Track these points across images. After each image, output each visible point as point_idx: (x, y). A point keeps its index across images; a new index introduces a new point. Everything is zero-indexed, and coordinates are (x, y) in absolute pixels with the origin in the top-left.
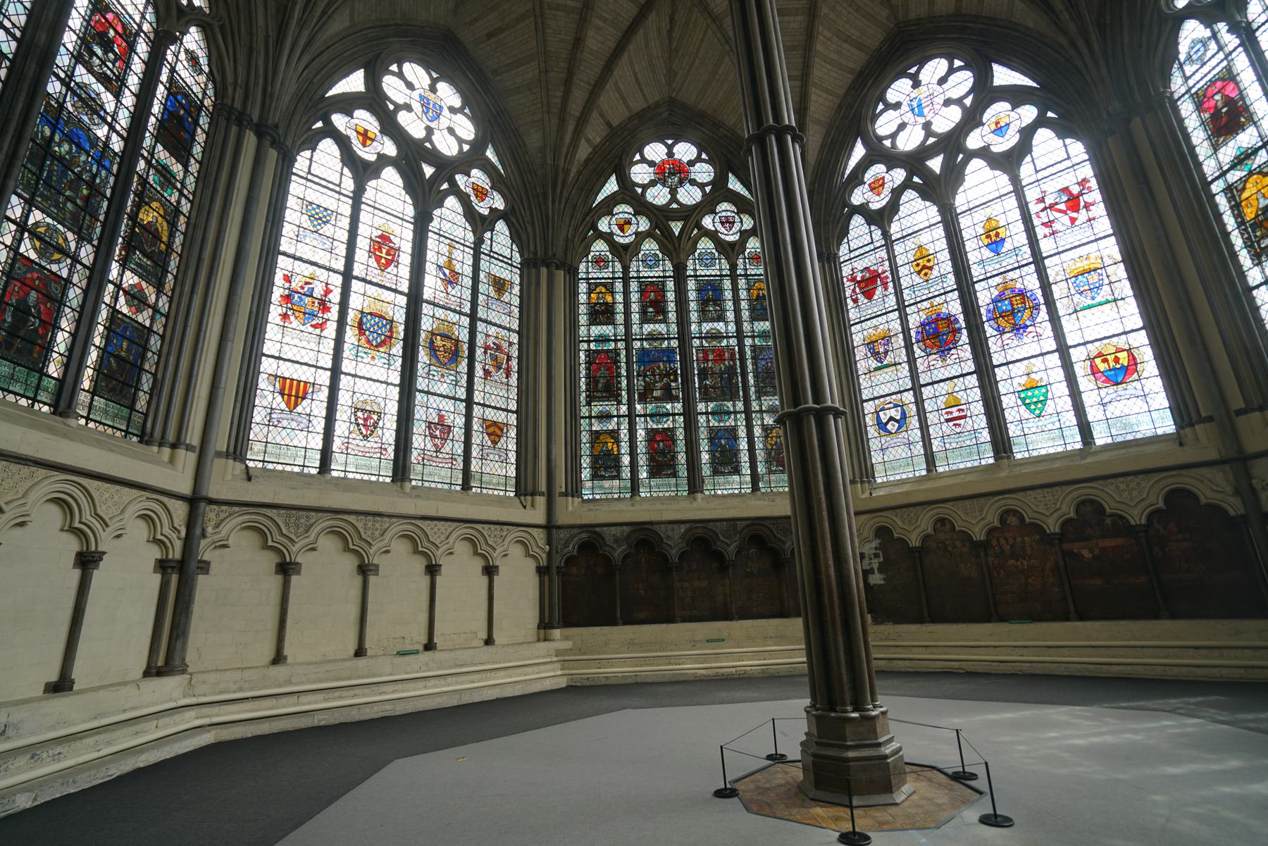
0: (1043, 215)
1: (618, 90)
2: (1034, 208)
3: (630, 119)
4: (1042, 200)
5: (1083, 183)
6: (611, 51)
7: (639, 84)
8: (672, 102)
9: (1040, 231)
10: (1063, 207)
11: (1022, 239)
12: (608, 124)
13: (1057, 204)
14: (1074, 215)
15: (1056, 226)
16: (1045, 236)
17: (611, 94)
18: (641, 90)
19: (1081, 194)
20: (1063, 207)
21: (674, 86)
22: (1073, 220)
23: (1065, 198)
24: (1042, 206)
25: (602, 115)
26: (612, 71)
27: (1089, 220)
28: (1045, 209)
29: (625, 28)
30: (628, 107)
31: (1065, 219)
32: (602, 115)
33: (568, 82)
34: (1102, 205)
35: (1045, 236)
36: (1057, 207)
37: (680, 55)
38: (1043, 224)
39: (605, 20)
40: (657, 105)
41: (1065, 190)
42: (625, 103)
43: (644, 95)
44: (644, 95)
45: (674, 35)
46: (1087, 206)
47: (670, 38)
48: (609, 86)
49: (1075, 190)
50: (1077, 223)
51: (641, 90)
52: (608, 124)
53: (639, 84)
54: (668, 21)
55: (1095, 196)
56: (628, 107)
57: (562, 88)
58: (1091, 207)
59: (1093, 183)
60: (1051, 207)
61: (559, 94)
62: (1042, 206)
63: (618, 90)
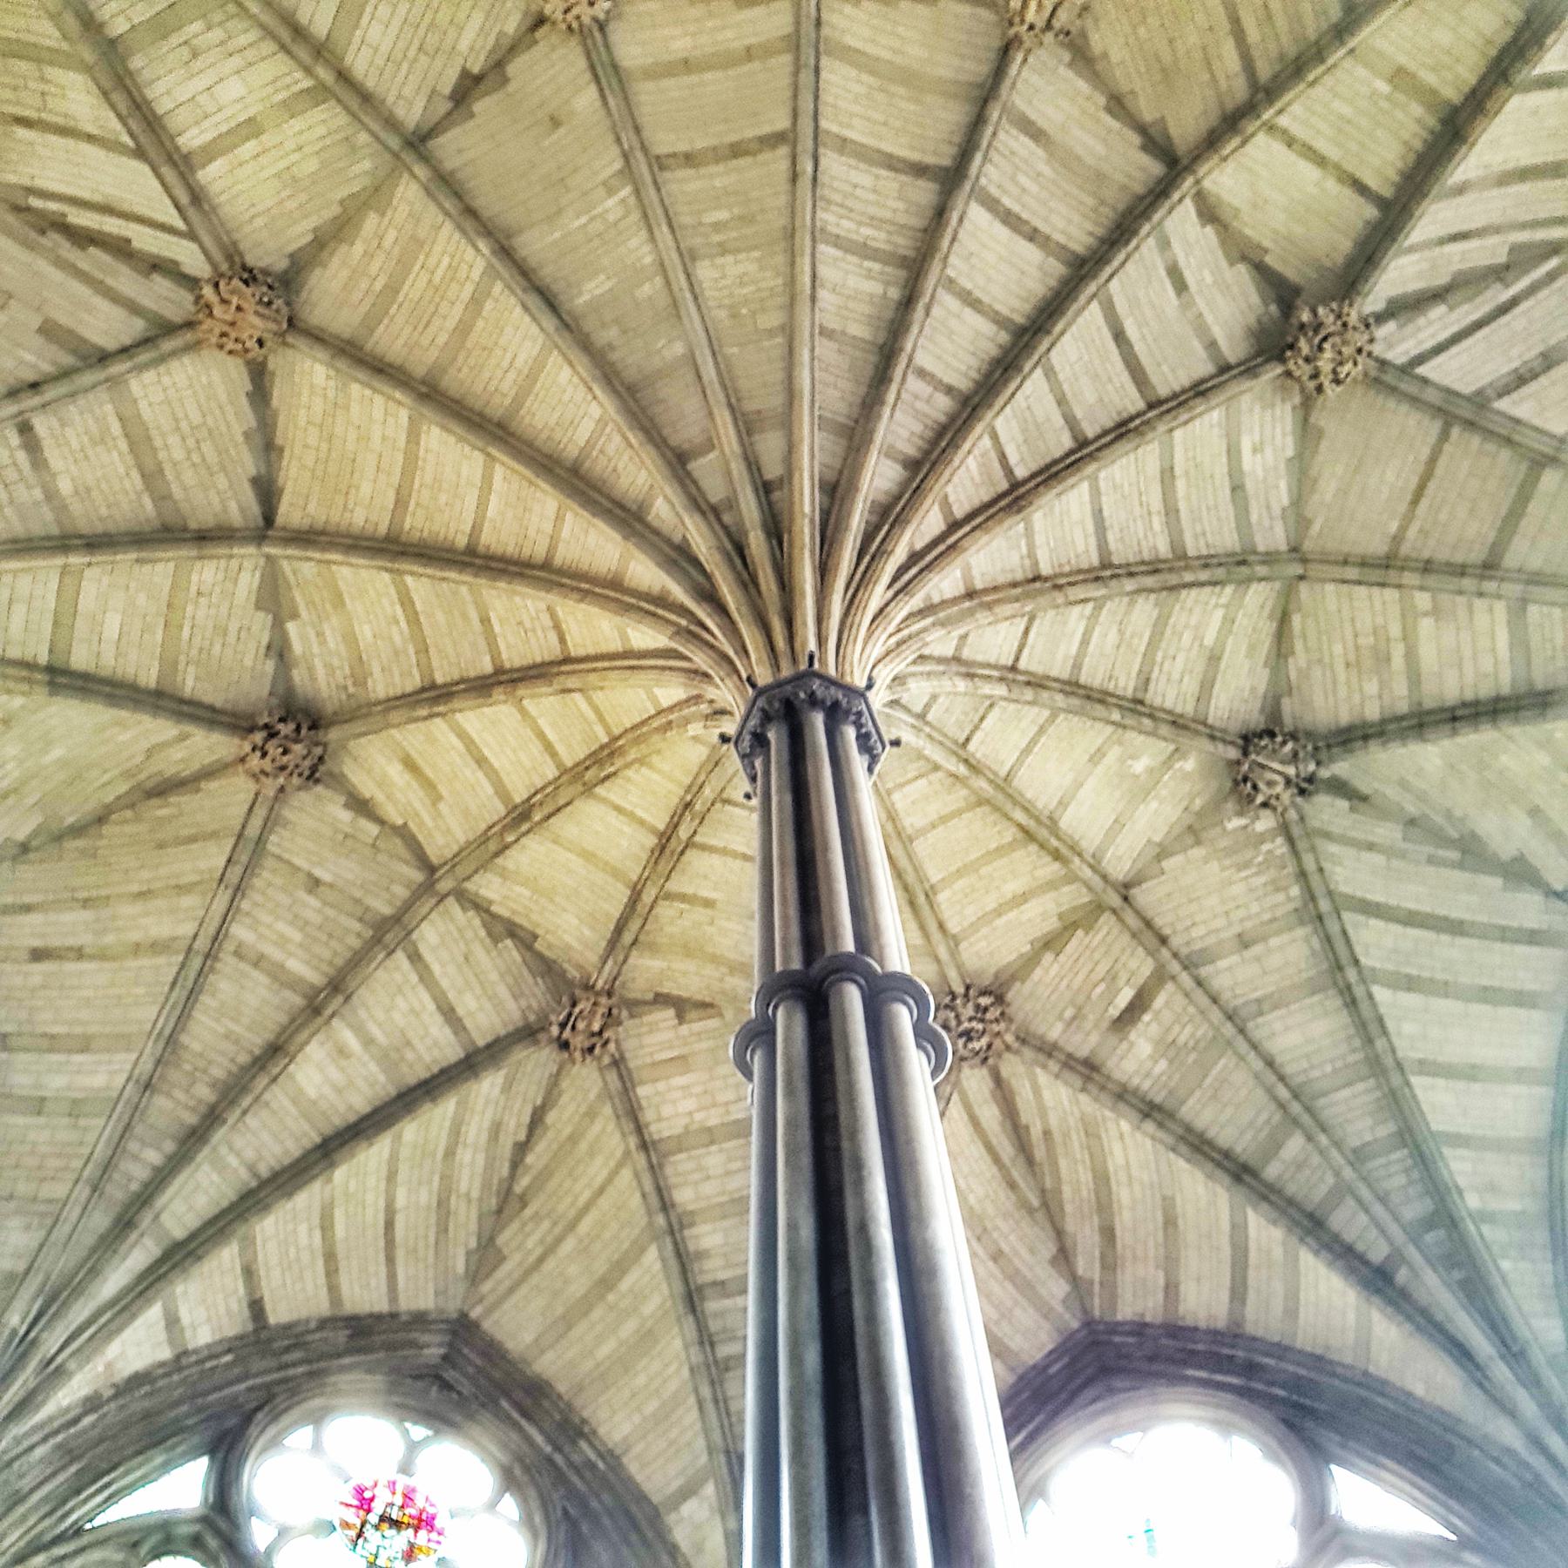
1: (326, 1225)
3: (323, 1323)
6: (352, 1118)
7: (390, 1243)
8: (463, 1329)
12: (256, 1308)
17: (303, 1229)
18: (390, 1260)
21: (486, 1287)
25: (249, 1273)
26: (332, 1165)
29: (412, 1080)
30: (333, 1289)
32: (249, 1273)
33: (193, 1139)
37: (528, 1212)
39: (368, 1042)
40: (420, 1319)
42: (331, 1272)
43: (392, 1277)
44: (392, 1277)
45: (530, 1159)
47: (516, 1163)
48: (307, 1199)
51: (390, 1260)
52: (256, 1308)
53: (390, 1243)
54: (526, 1119)
56: (333, 1289)
57: (170, 1146)
61: (154, 1157)
63: (326, 1225)
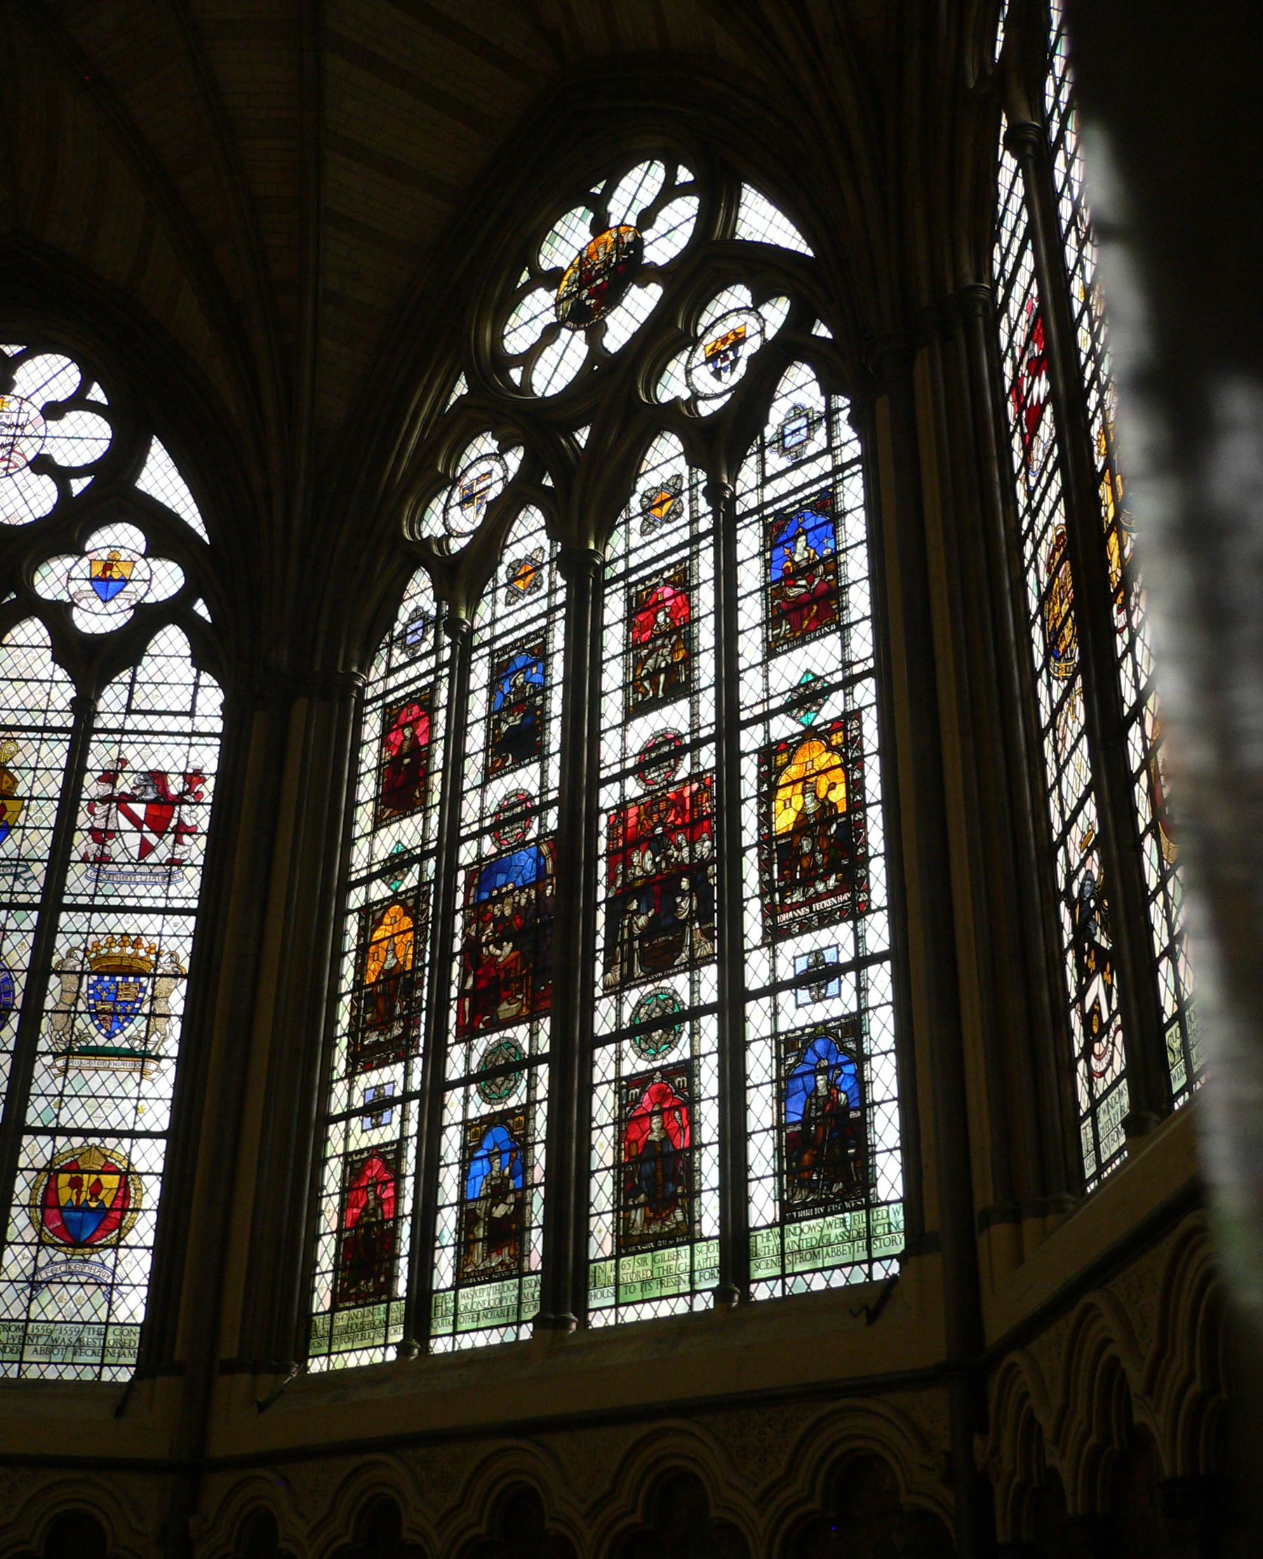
0: (100, 810)
2: (92, 787)
4: (109, 777)
5: (193, 778)
9: (82, 844)
10: (139, 809)
11: (41, 844)
13: (133, 799)
14: (152, 838)
15: (114, 848)
16: (85, 860)
19: (180, 800)
20: (139, 809)
22: (146, 848)
23: (151, 795)
24: (105, 789)
27: (172, 862)
28: (106, 800)
31: (133, 840)
34: (202, 841)
35: (85, 860)
36: (133, 806)
38: (92, 830)
41: (157, 778)
46: (182, 830)
49: (175, 786)
50: (152, 859)
55: (200, 817)
58: (186, 838)
59: (208, 788)
60: (122, 801)
62: (105, 789)
